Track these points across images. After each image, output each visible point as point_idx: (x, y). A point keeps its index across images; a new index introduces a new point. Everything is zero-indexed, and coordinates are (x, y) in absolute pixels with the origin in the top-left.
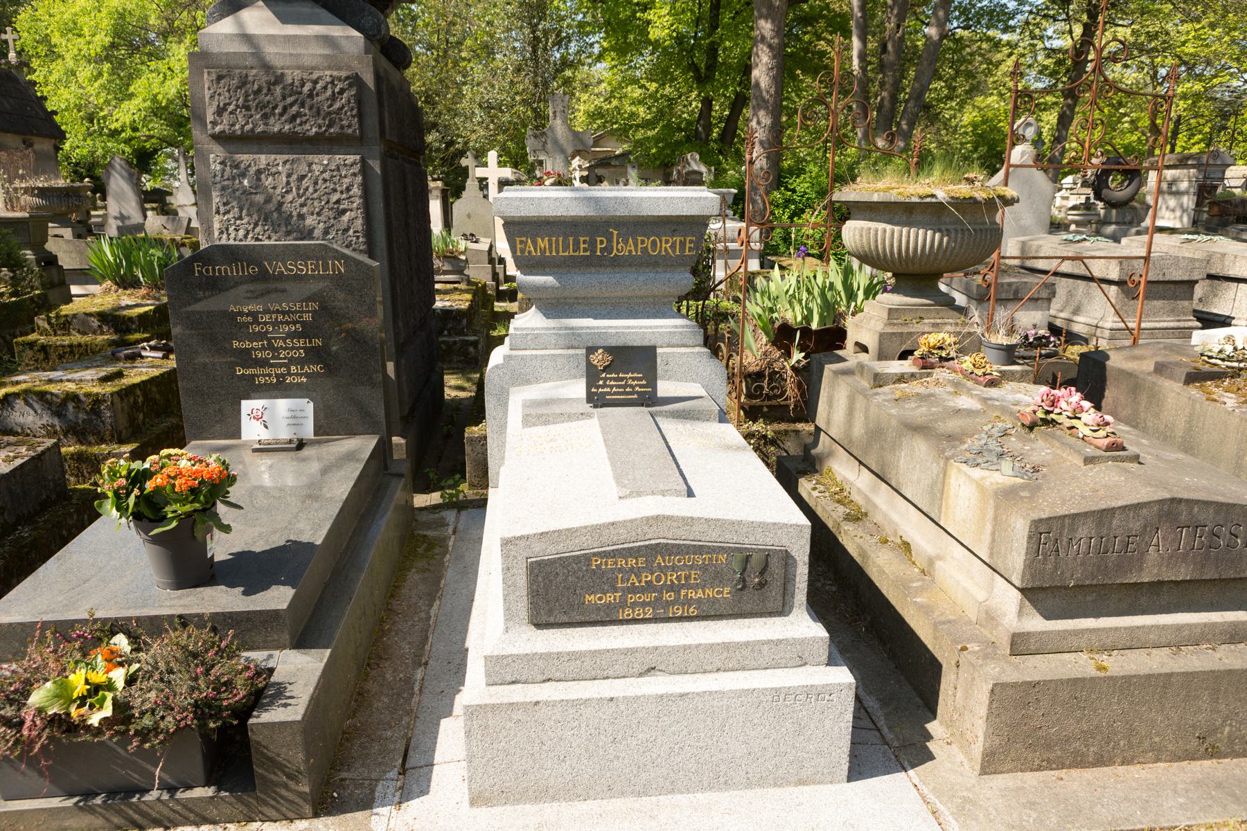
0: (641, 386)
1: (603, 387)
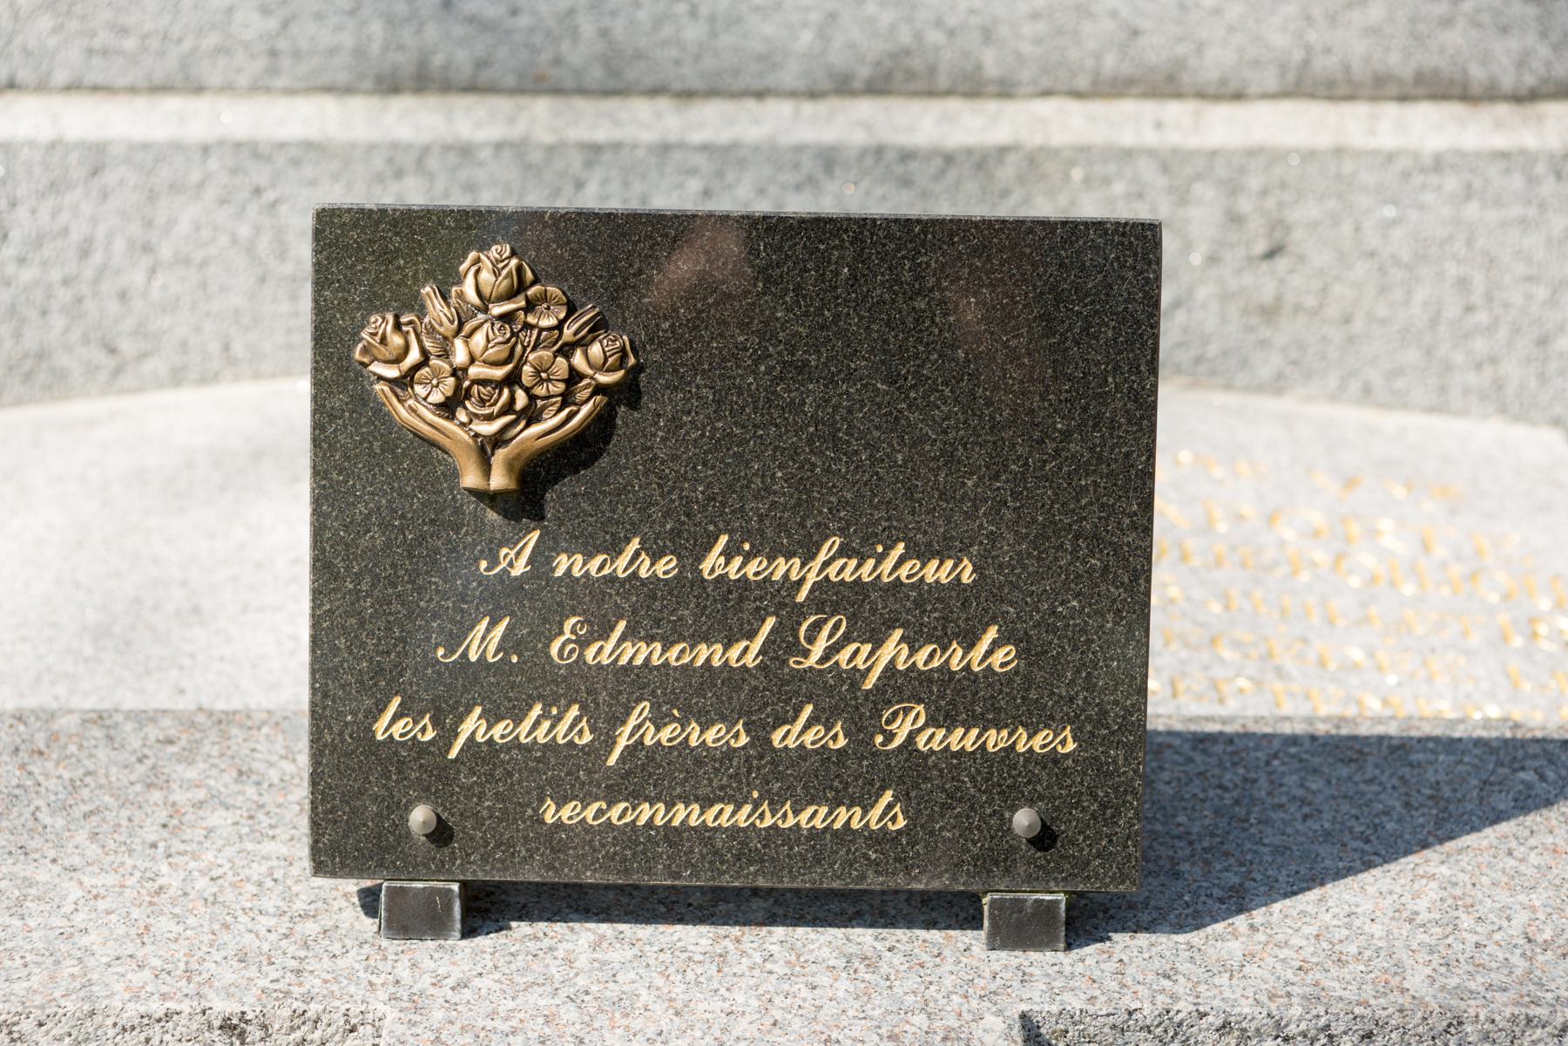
0: (953, 699)
1: (507, 689)
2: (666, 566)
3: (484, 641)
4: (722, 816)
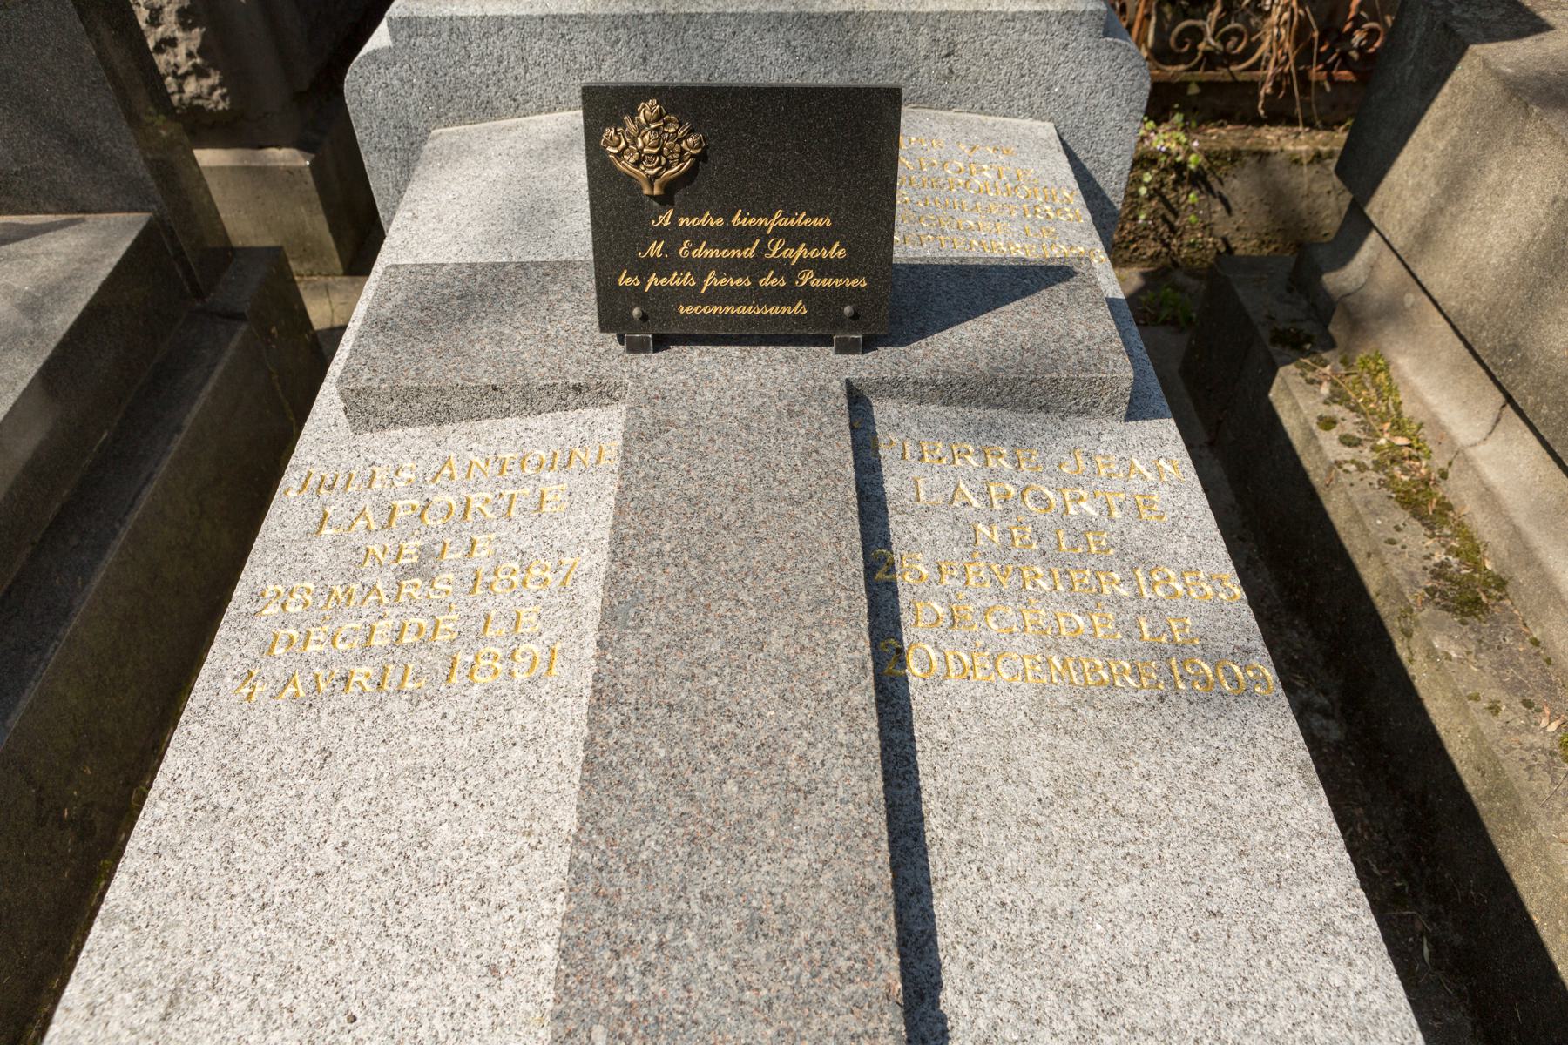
1: (664, 266)
2: (720, 221)
3: (655, 249)
4: (742, 310)
